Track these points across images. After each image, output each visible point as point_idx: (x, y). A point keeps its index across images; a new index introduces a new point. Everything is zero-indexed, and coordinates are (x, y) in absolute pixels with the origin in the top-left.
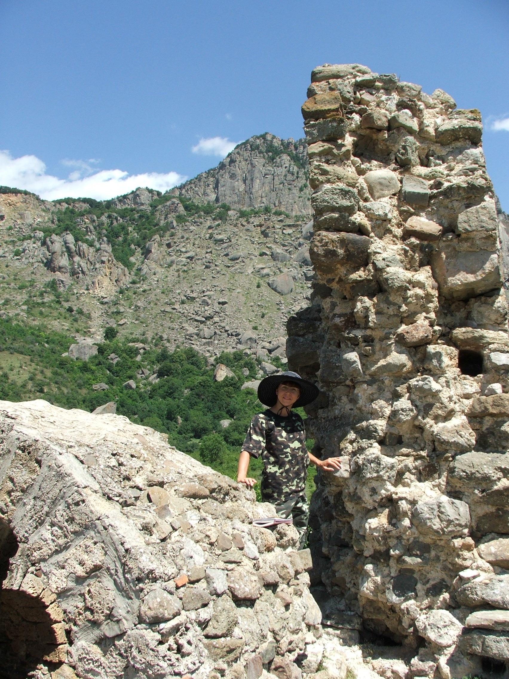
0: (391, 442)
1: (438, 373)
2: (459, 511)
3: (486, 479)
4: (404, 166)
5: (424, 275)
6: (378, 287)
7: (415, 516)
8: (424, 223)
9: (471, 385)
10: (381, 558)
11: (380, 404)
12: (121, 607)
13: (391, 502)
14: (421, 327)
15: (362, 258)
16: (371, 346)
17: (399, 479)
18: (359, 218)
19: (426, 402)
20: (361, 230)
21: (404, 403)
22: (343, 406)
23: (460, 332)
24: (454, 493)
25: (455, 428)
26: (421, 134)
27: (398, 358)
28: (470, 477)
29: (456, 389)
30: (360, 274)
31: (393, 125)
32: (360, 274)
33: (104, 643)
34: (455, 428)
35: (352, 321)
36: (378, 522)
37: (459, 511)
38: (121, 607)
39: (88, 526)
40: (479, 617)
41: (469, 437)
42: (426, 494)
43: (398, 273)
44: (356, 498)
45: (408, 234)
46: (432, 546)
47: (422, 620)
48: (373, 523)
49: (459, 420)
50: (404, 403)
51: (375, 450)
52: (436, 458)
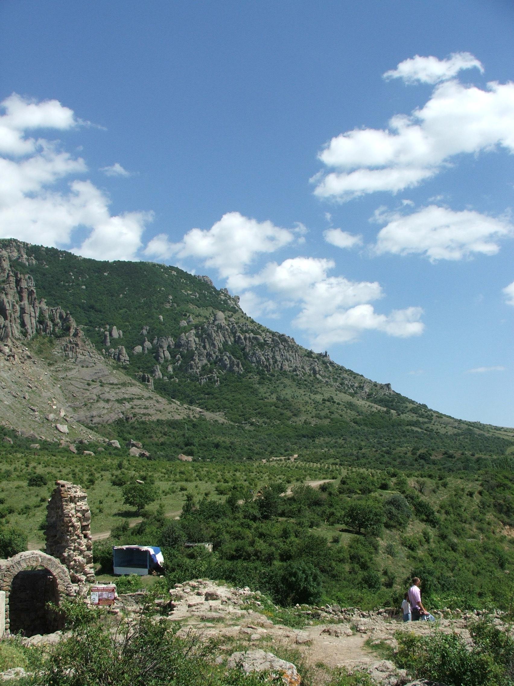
0: (74, 551)
1: (81, 539)
2: (85, 560)
3: (89, 556)
4: (76, 504)
5: (79, 523)
6: (73, 526)
7: (79, 562)
8: (79, 514)
9: (85, 540)
10: (73, 568)
11: (73, 544)
12: (63, 575)
13: (75, 560)
14: (79, 531)
15: (71, 521)
16: (72, 535)
17: (76, 556)
18: (70, 515)
19: (80, 544)
20: (70, 517)
21: (76, 544)
22: (64, 544)
23: (84, 532)
24: (84, 558)
25: (84, 548)
26: (78, 497)
27: (76, 537)
28: (87, 555)
29: (84, 541)
30: (70, 524)
31: (75, 497)
32: (70, 524)
33: (61, 580)
34: (84, 548)
35: (68, 531)
36: (72, 563)
37: (85, 560)
38: (63, 575)
39: (59, 567)
40: (88, 575)
41: (86, 549)
42: (80, 558)
43: (76, 524)
44: (68, 559)
45: (77, 517)
46: (82, 566)
47: (79, 577)
48: (72, 563)
49: (84, 546)
50: (76, 544)
51: (72, 552)
52: (81, 552)
